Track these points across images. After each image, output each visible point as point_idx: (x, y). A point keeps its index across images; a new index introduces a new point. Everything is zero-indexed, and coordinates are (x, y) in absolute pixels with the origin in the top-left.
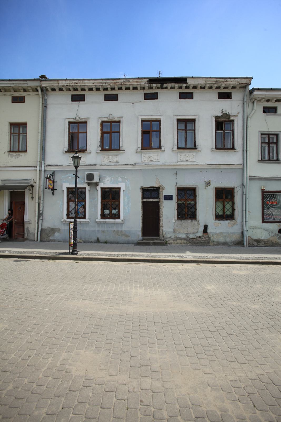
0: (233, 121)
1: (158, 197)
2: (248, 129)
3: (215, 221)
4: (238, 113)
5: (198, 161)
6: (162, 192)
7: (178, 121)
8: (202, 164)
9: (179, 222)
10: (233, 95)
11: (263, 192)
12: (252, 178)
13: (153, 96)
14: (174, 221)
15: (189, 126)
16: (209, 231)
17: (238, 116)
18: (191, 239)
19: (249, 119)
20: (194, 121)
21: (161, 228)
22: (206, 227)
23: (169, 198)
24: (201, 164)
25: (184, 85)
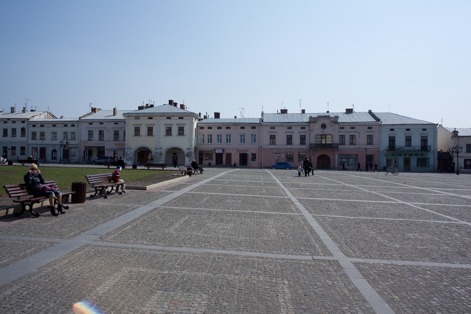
11: (32, 148)
22: (18, 157)
23: (9, 149)
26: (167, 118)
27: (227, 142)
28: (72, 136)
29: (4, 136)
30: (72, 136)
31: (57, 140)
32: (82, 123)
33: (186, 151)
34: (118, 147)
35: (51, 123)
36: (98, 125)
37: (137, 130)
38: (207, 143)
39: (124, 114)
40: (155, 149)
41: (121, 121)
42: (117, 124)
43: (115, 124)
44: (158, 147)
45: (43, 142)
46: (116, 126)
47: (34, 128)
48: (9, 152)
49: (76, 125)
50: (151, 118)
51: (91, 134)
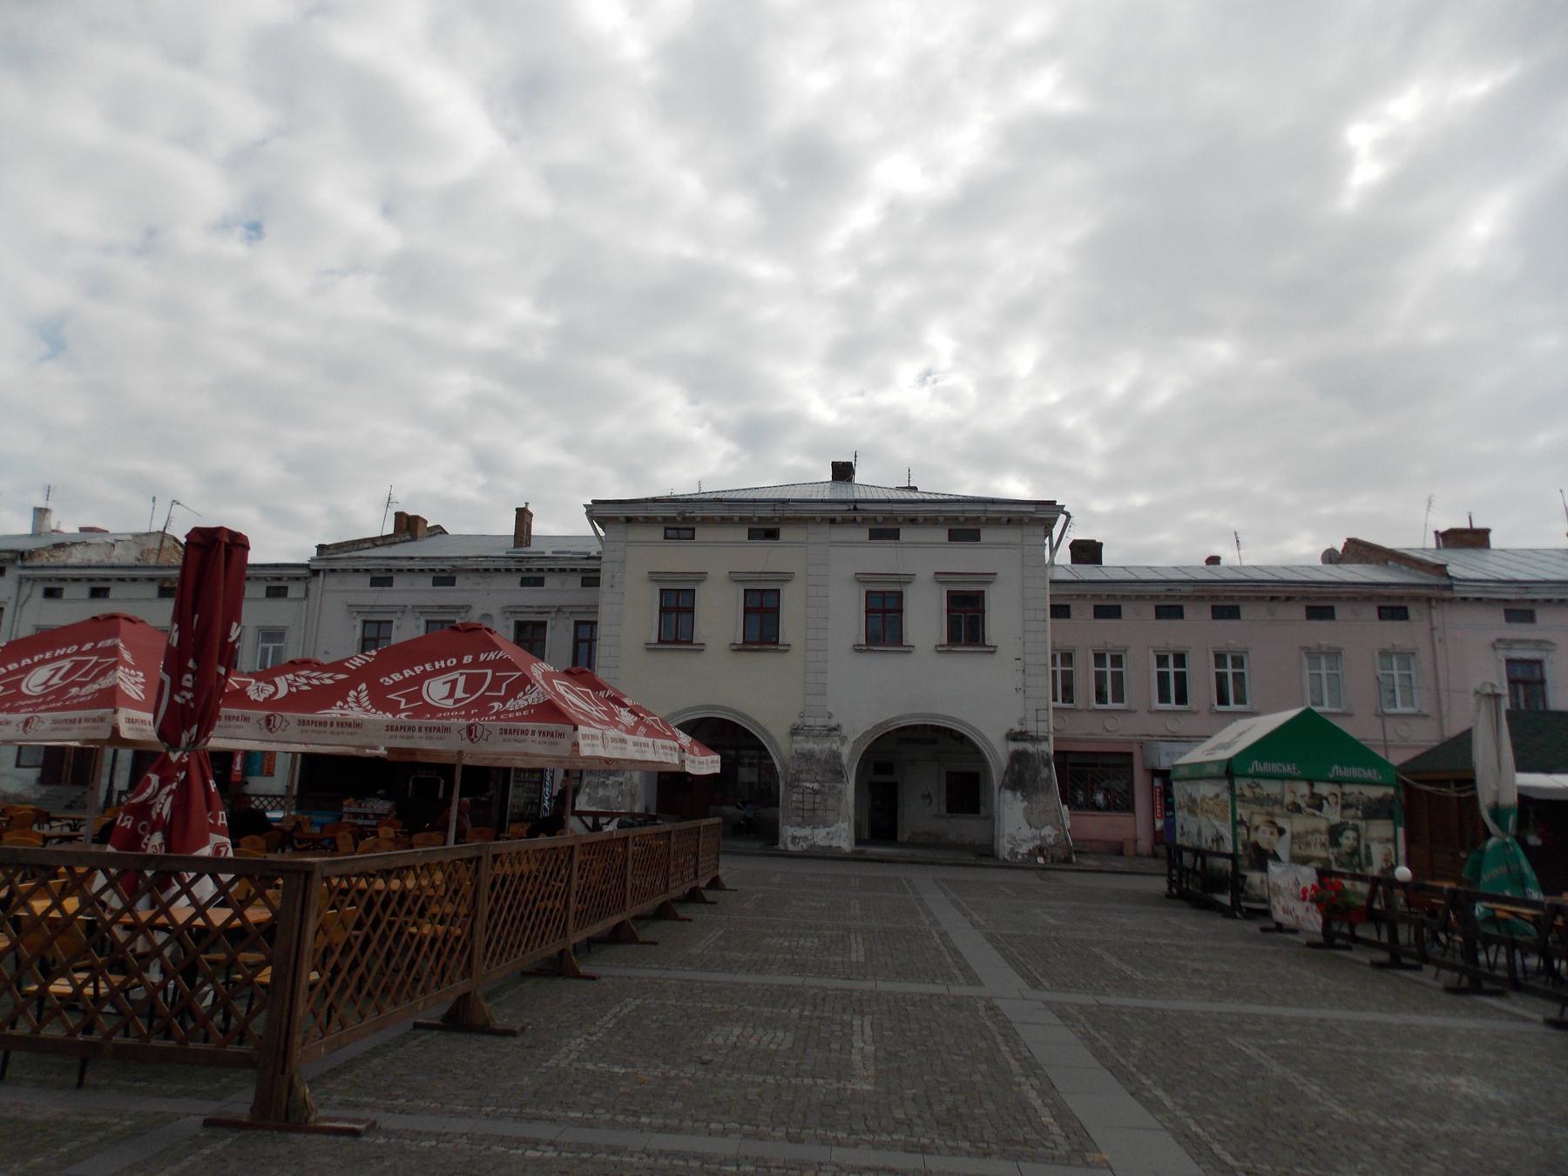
4: (10, 598)
26: (876, 535)
27: (1223, 700)
28: (265, 651)
30: (265, 651)
32: (332, 582)
33: (999, 753)
35: (151, 580)
37: (678, 610)
38: (1094, 704)
39: (601, 512)
40: (795, 731)
42: (539, 582)
43: (525, 582)
44: (809, 721)
49: (295, 590)
50: (772, 534)
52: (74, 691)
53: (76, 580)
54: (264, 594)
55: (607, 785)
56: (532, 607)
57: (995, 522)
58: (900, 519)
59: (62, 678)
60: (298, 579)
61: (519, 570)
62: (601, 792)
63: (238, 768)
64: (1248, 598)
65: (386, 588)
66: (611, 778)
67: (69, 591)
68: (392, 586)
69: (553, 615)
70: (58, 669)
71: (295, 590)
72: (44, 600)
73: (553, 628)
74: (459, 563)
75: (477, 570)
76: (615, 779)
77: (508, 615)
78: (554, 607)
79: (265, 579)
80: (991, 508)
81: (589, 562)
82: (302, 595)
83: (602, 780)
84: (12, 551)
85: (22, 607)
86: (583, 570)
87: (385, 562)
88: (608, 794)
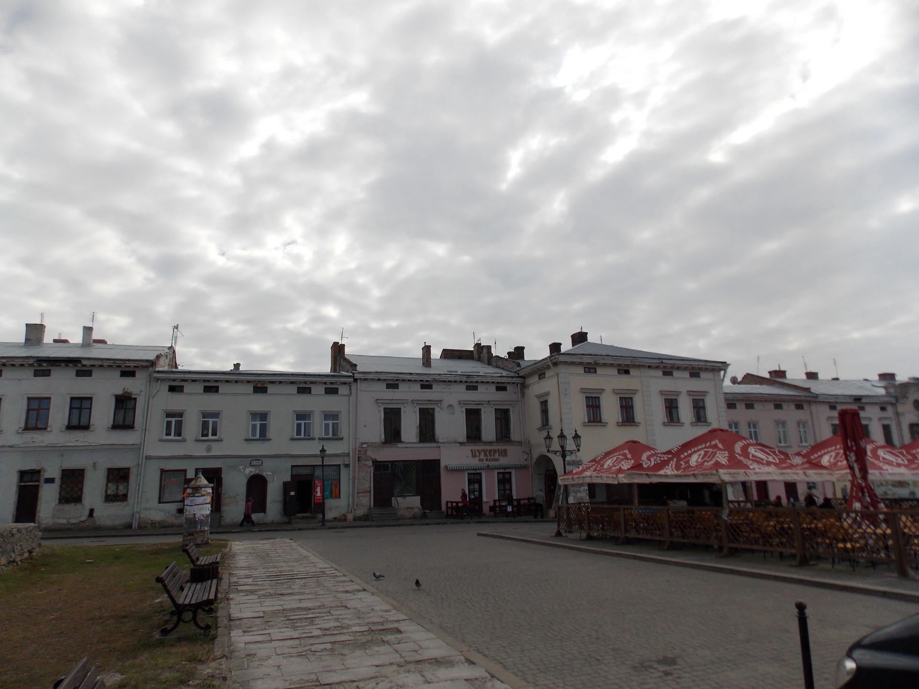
0: (135, 399)
1: (38, 481)
2: (150, 408)
3: (104, 504)
4: (141, 392)
5: (89, 441)
6: (43, 475)
7: (72, 399)
8: (94, 444)
9: (61, 507)
10: (137, 374)
12: (148, 458)
13: (46, 373)
14: (54, 505)
15: (86, 404)
16: (94, 515)
17: (140, 395)
18: (73, 524)
19: (151, 398)
20: (91, 399)
21: (38, 514)
22: (92, 511)
23: (50, 481)
24: (92, 444)
25: (79, 365)
28: (327, 426)
29: (27, 428)
31: (270, 440)
34: (480, 460)
35: (249, 382)
36: (414, 392)
41: (488, 382)
42: (475, 388)
43: (468, 388)
45: (209, 449)
46: (472, 396)
47: (176, 397)
48: (48, 496)
49: (343, 390)
50: (627, 372)
51: (392, 418)
52: (706, 464)
53: (194, 381)
54: (324, 393)
55: (581, 491)
56: (475, 401)
57: (706, 370)
58: (676, 367)
59: (702, 459)
60: (345, 383)
61: (466, 382)
62: (579, 495)
63: (319, 494)
64: (756, 401)
65: (396, 390)
66: (582, 488)
67: (188, 388)
68: (398, 389)
69: (485, 405)
70: (700, 455)
71: (343, 390)
72: (170, 393)
73: (485, 412)
74: (437, 377)
75: (445, 381)
76: (584, 488)
77: (462, 405)
78: (486, 401)
79: (325, 383)
80: (708, 364)
81: (503, 379)
82: (347, 392)
83: (578, 489)
84: (147, 361)
85: (153, 397)
86: (498, 383)
87: (398, 375)
88: (581, 495)
